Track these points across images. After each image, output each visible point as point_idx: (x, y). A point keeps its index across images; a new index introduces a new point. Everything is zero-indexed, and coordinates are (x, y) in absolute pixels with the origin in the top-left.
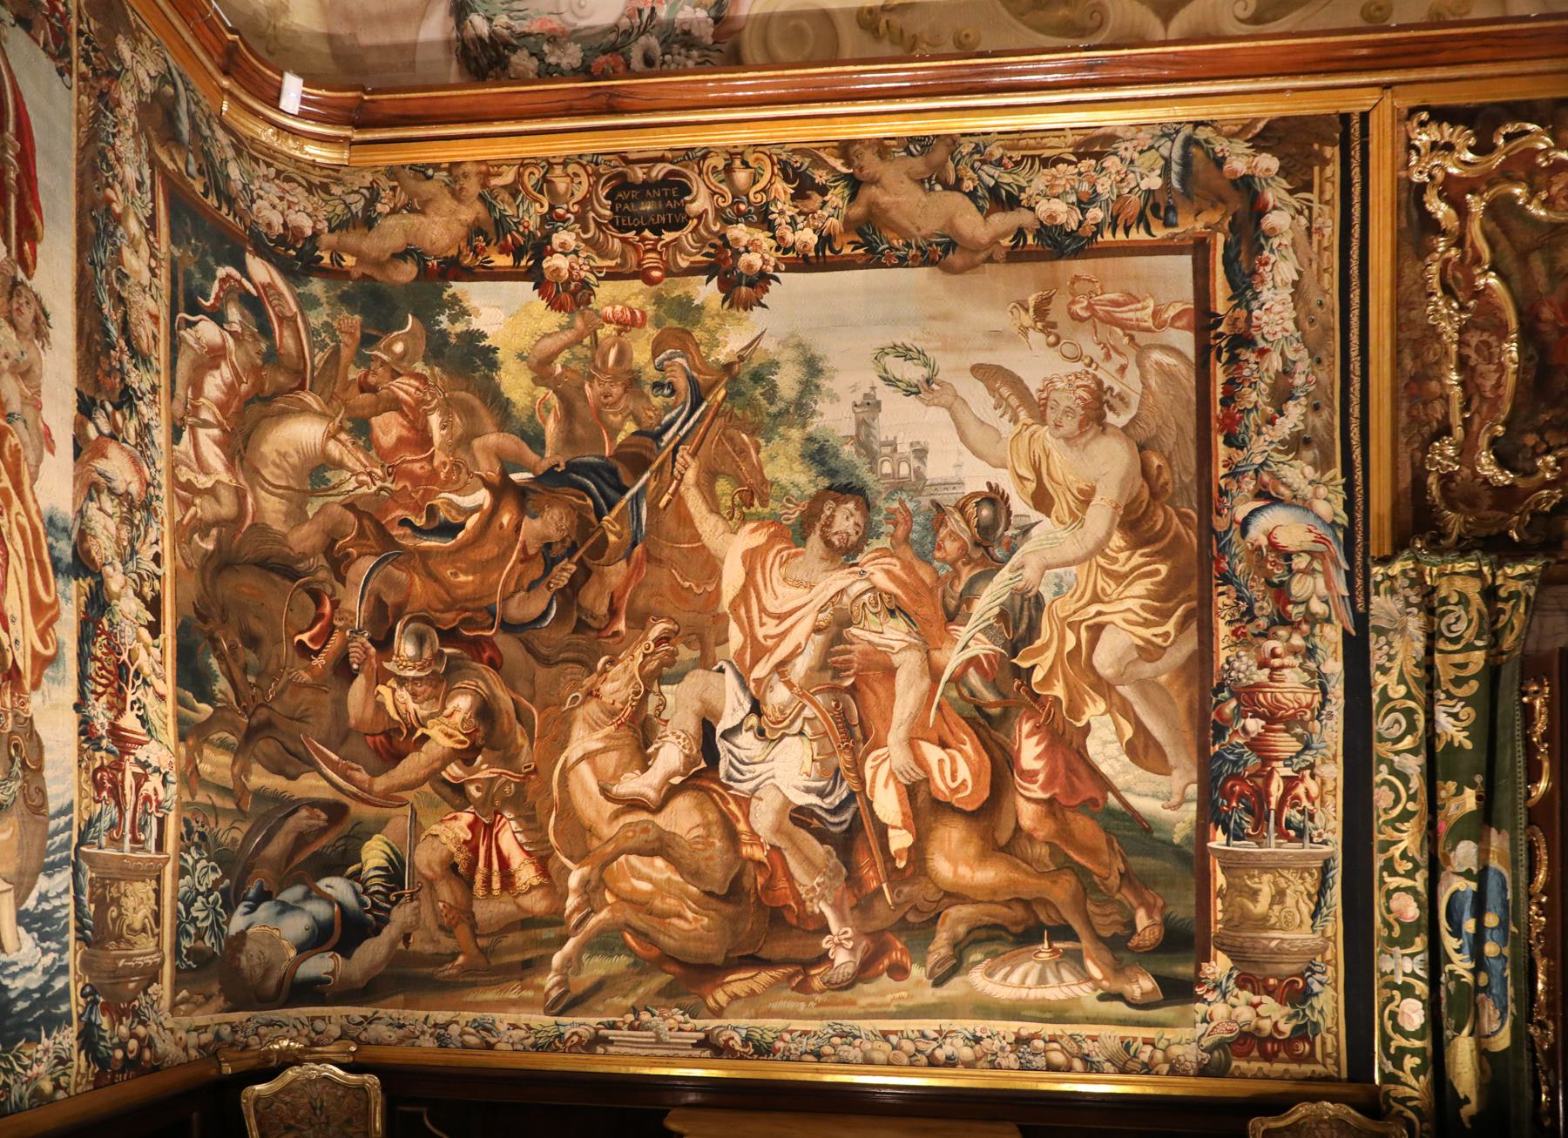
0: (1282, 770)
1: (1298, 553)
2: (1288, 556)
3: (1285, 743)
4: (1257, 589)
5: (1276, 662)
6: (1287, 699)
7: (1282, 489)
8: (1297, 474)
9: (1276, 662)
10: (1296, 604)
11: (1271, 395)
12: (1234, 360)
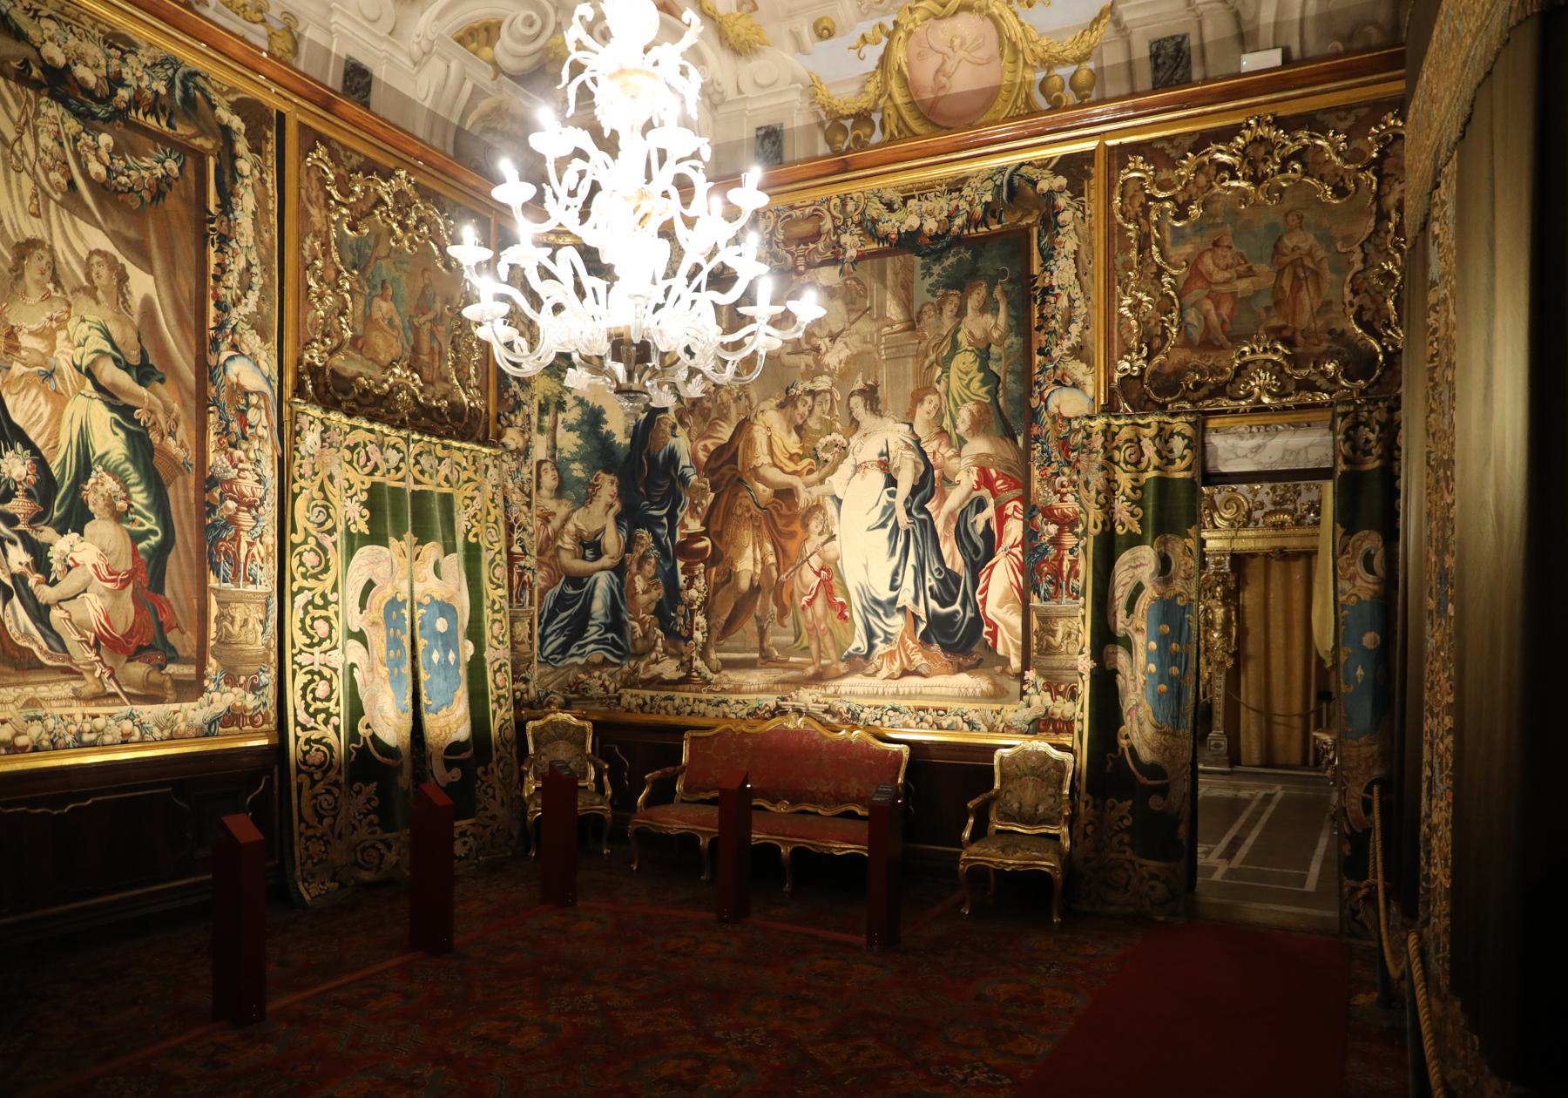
0: (245, 538)
1: (252, 393)
2: (247, 394)
3: (245, 518)
4: (231, 413)
5: (241, 466)
6: (247, 492)
7: (244, 346)
8: (252, 341)
9: (241, 466)
10: (251, 427)
11: (240, 282)
12: (220, 250)
